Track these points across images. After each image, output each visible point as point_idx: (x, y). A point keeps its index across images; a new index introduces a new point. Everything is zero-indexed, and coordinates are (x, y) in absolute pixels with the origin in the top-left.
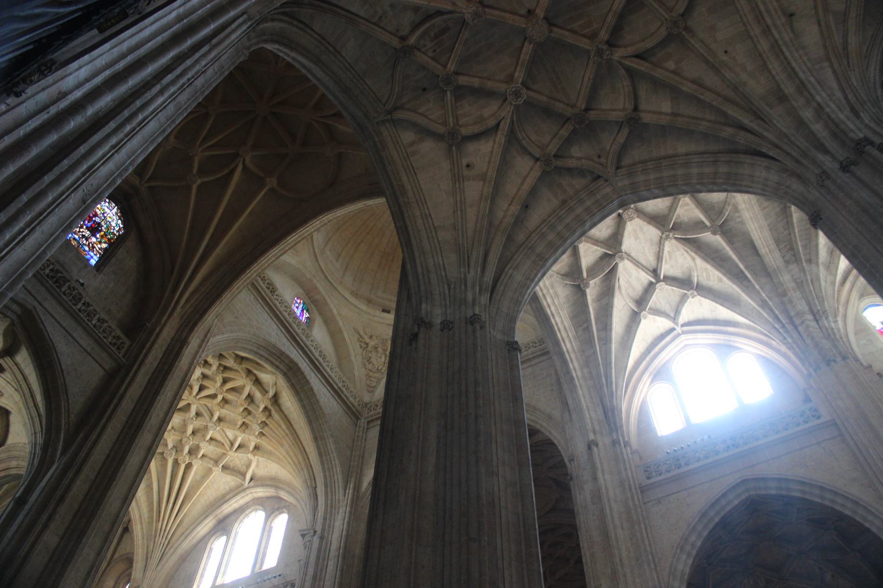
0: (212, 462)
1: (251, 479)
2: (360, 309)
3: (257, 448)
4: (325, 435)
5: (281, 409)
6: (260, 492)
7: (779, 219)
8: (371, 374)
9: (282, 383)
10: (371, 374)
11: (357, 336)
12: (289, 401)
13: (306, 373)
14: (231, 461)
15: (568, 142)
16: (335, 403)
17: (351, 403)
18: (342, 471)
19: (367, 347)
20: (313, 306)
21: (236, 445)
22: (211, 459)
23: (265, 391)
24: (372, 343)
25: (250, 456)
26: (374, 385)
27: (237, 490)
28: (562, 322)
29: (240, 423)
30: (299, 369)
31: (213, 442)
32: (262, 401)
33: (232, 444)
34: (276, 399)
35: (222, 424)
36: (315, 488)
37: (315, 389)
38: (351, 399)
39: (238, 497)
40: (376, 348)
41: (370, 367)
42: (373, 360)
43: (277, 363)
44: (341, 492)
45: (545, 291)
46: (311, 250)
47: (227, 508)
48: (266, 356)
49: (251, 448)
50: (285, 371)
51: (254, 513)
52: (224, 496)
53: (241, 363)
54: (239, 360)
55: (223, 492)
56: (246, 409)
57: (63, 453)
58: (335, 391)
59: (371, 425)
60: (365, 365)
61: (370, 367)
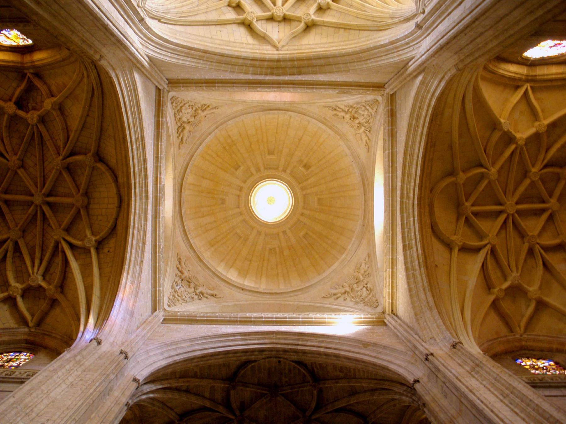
2: (232, 119)
4: (201, 62)
5: (234, 23)
9: (268, 52)
10: (182, 104)
11: (215, 105)
30: (272, 74)
34: (248, 26)
36: (159, 21)
40: (194, 117)
43: (296, 63)
44: (151, 53)
48: (314, 62)
50: (282, 63)
53: (306, 24)
54: (309, 24)
61: (187, 105)
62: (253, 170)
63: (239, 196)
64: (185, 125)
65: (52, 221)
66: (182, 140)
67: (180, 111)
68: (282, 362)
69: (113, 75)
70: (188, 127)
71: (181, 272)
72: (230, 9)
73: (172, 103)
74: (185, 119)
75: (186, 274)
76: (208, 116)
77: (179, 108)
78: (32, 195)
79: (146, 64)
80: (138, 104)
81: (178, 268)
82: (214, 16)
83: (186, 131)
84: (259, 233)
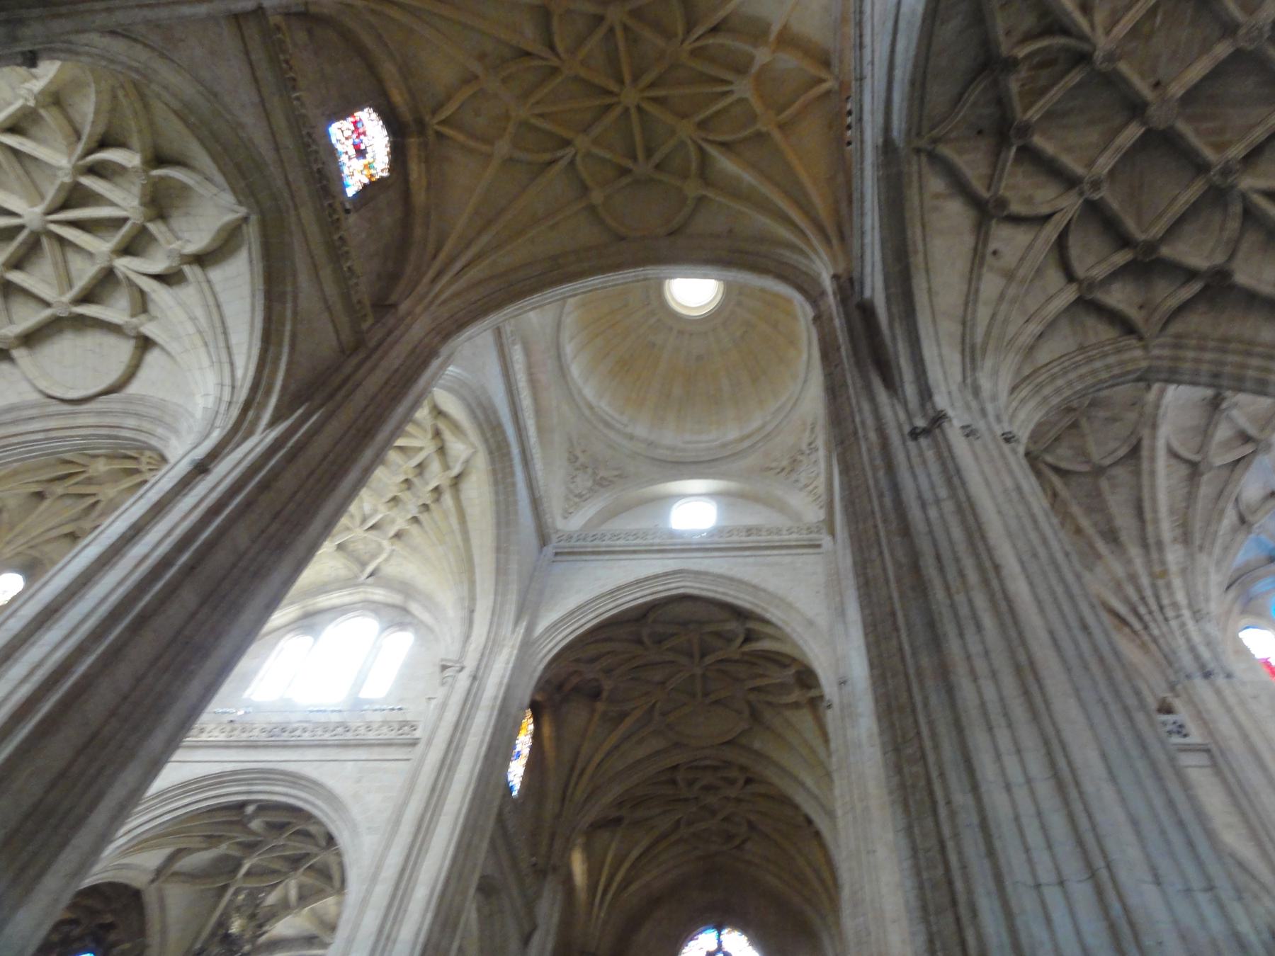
1: (371, 575)
3: (398, 536)
6: (379, 594)
9: (481, 462)
12: (478, 491)
14: (353, 542)
15: (1116, 275)
19: (575, 462)
21: (370, 524)
23: (447, 467)
24: (582, 459)
25: (386, 543)
27: (348, 583)
29: (390, 495)
32: (436, 476)
33: (364, 520)
34: (457, 481)
39: (344, 592)
40: (587, 467)
42: (578, 480)
44: (510, 628)
47: (323, 601)
49: (392, 533)
51: (359, 619)
56: (407, 481)
57: (273, 423)
59: (559, 558)
61: (572, 486)
62: (652, 320)
63: (691, 335)
64: (598, 478)
65: (721, 655)
66: (616, 476)
67: (580, 496)
69: (541, 667)
70: (602, 473)
71: (783, 469)
72: (442, 499)
74: (589, 484)
75: (785, 463)
78: (693, 676)
79: (524, 624)
81: (779, 473)
82: (454, 521)
84: (739, 304)
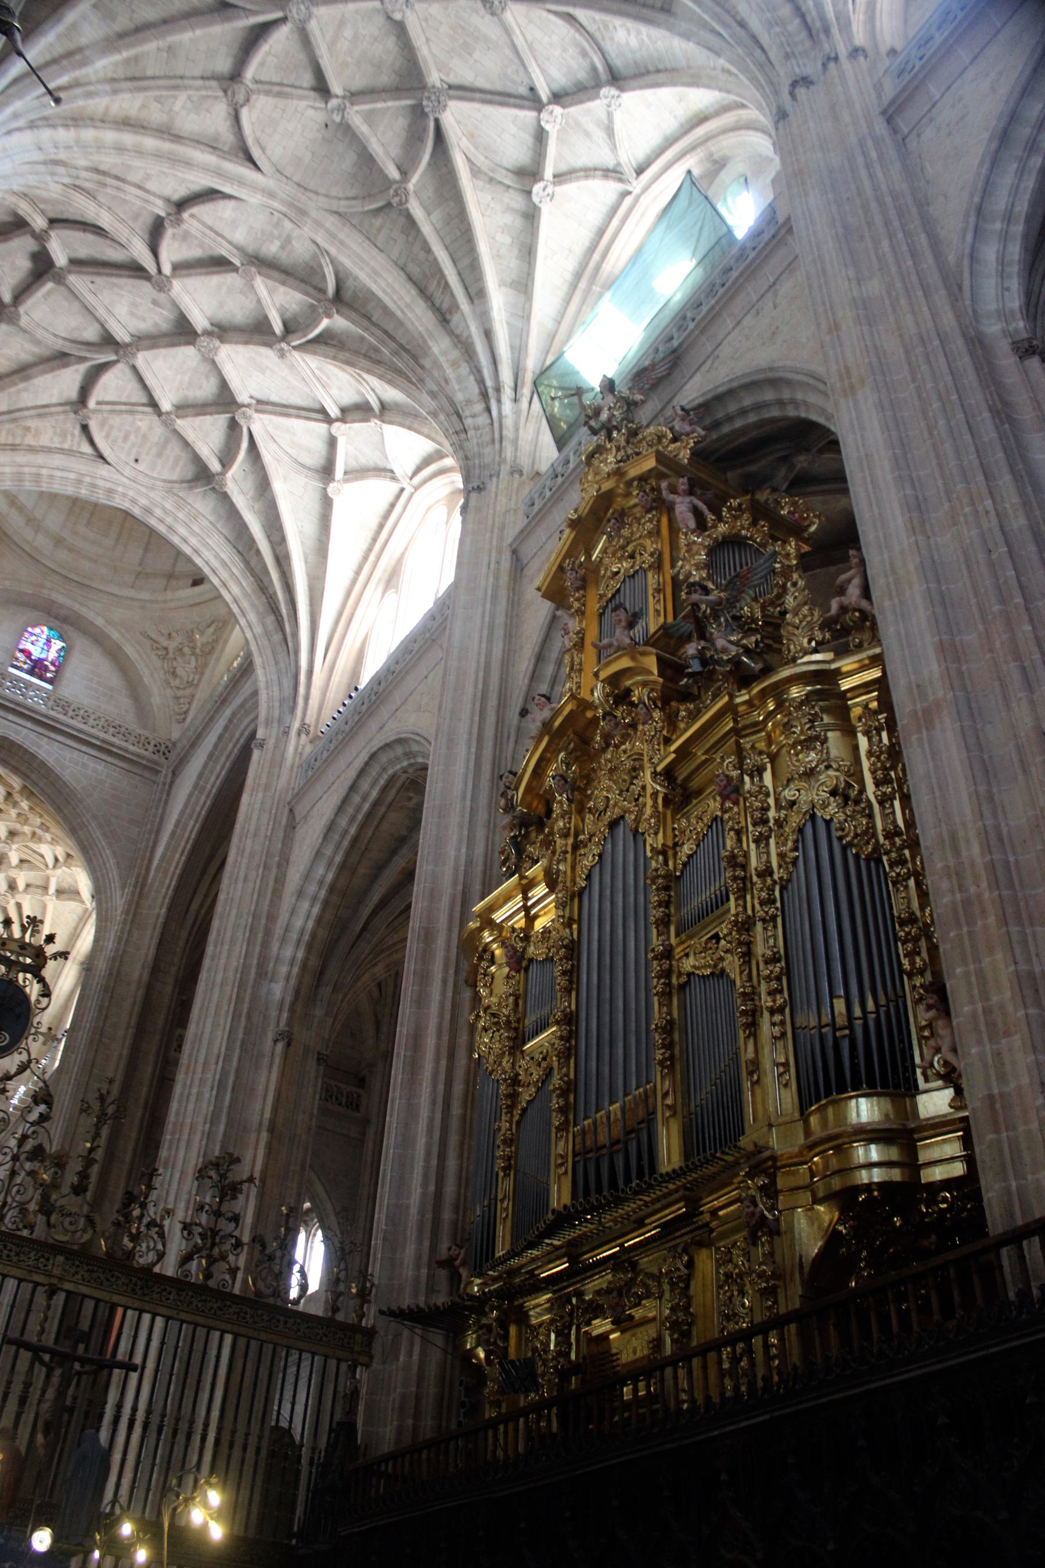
0: (39, 891)
7: (410, 239)
8: (179, 693)
13: (27, 745)
16: (100, 767)
17: (133, 754)
18: (118, 863)
20: (66, 627)
22: (38, 887)
24: (172, 645)
26: (185, 708)
28: (217, 556)
30: (12, 743)
31: (26, 865)
35: (16, 839)
37: (51, 762)
38: (131, 748)
41: (177, 682)
42: (180, 671)
44: (119, 893)
45: (169, 520)
46: (19, 551)
52: (76, 929)
55: (73, 924)
58: (100, 749)
60: (168, 683)
61: (177, 682)
67: (190, 684)
68: (133, 458)
69: (164, 910)
73: (186, 712)
76: (166, 632)
77: (188, 692)
80: (173, 833)
83: (204, 640)
